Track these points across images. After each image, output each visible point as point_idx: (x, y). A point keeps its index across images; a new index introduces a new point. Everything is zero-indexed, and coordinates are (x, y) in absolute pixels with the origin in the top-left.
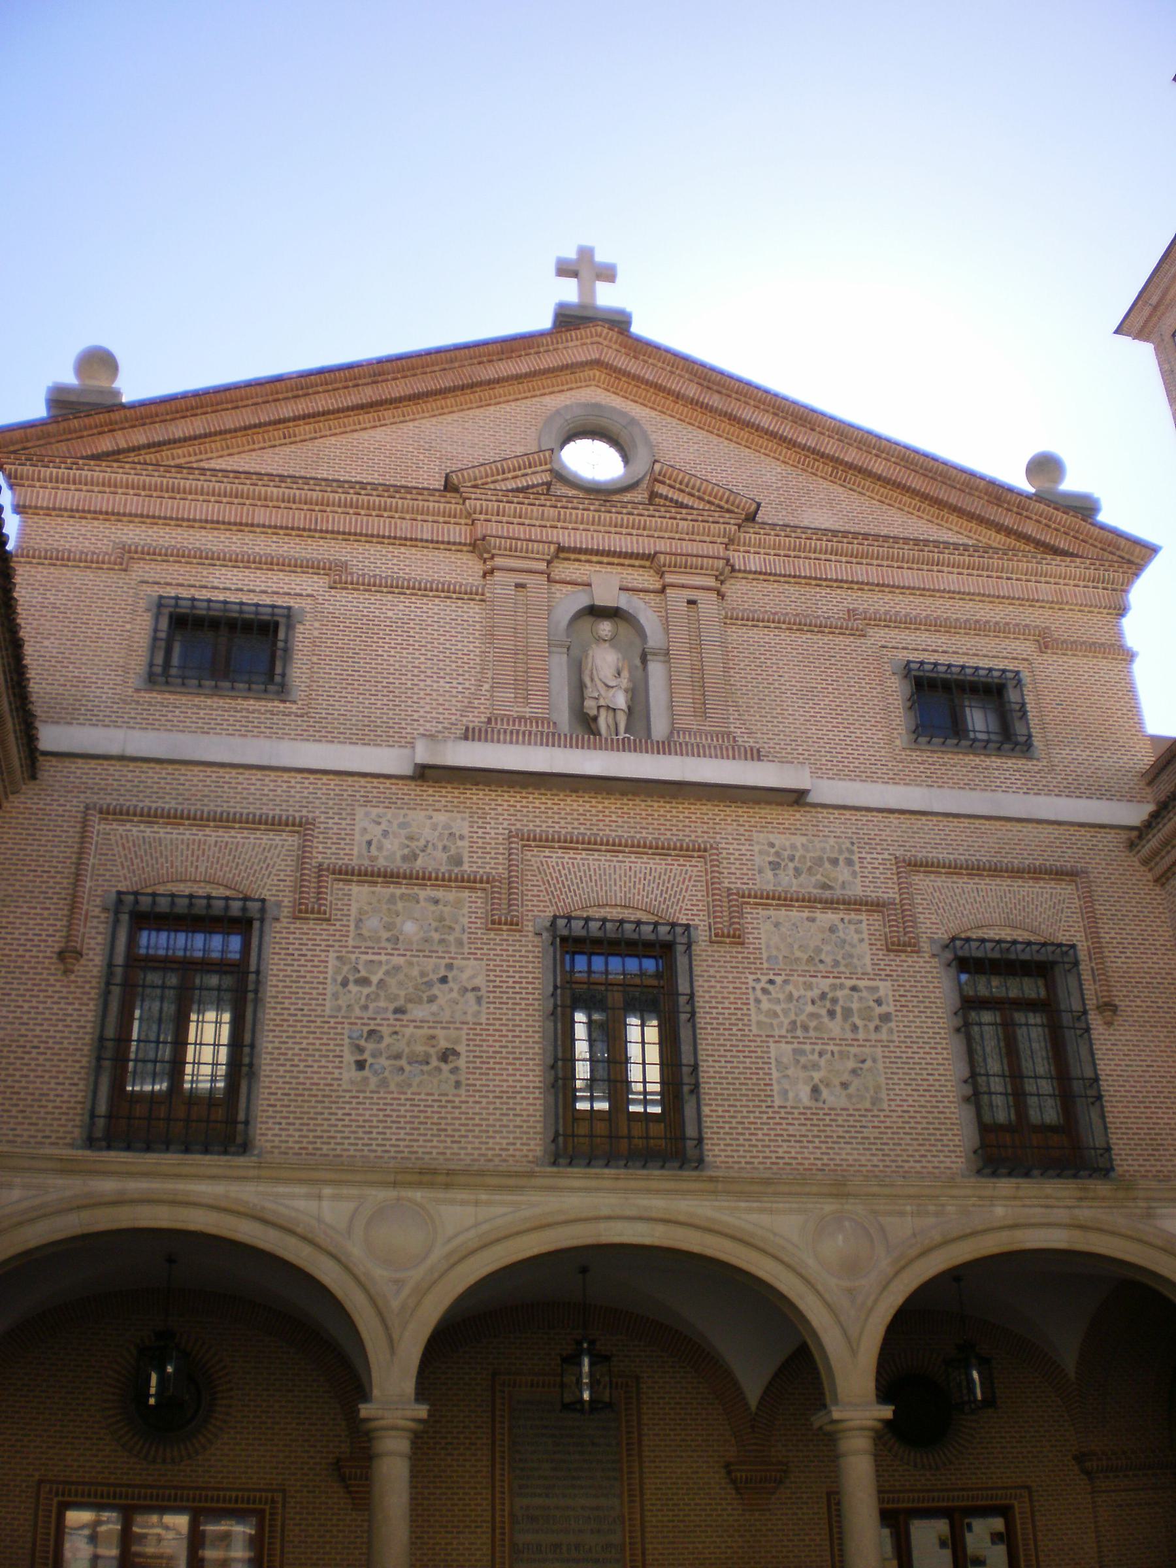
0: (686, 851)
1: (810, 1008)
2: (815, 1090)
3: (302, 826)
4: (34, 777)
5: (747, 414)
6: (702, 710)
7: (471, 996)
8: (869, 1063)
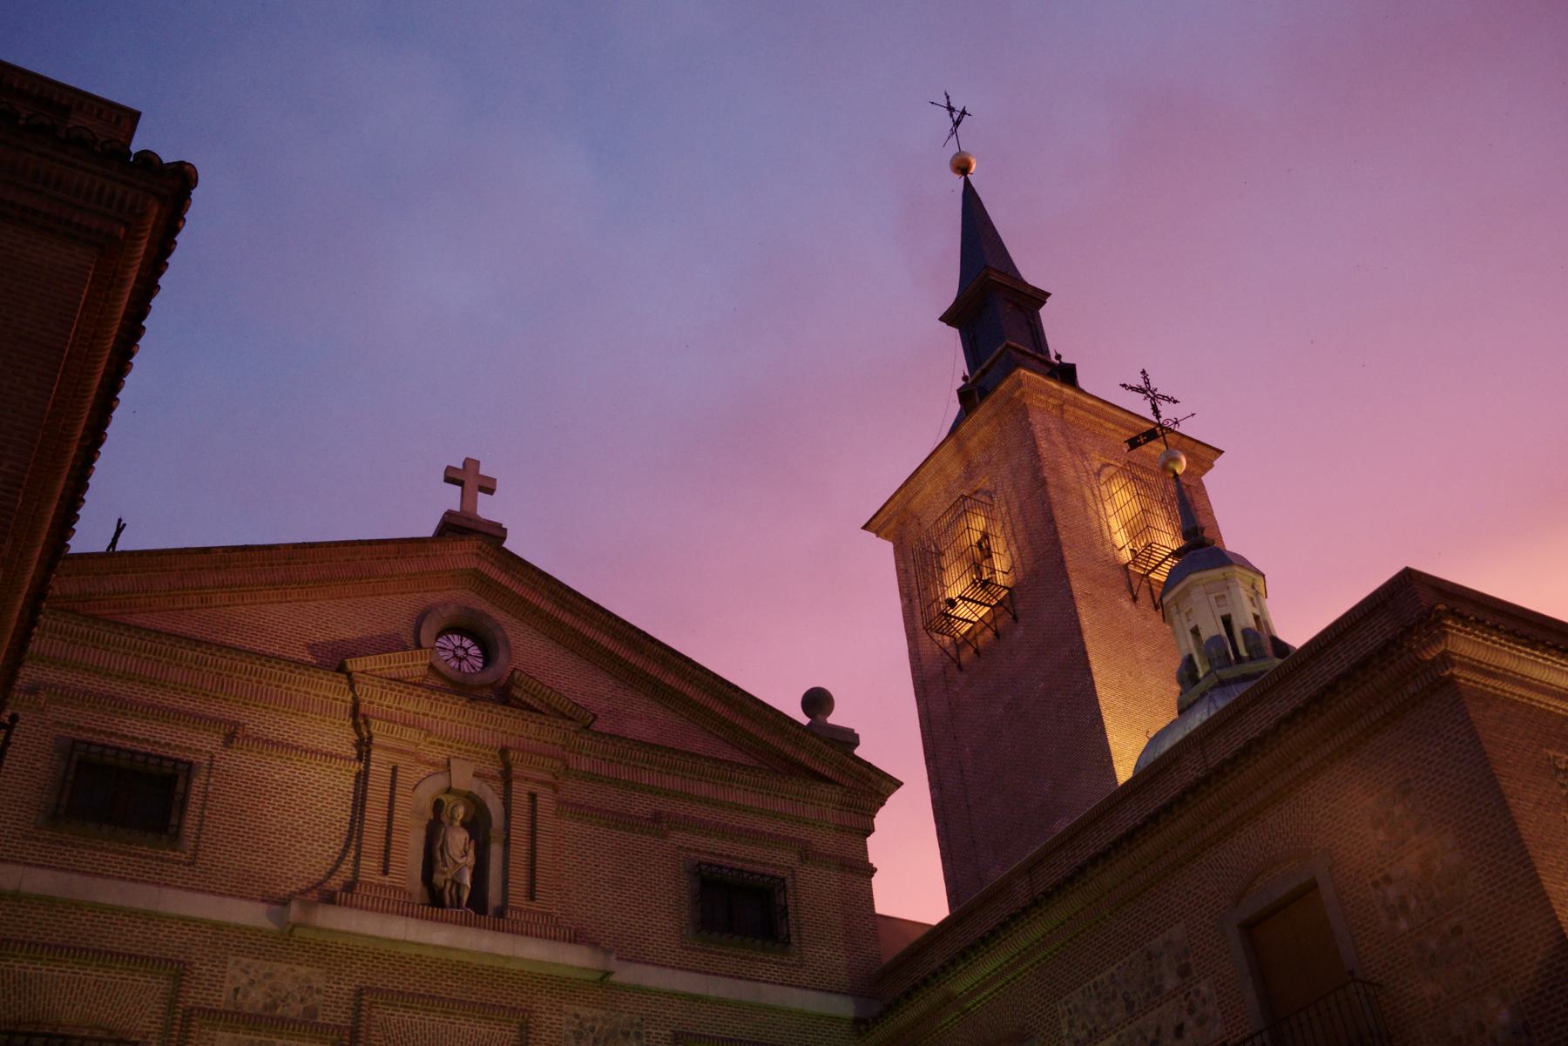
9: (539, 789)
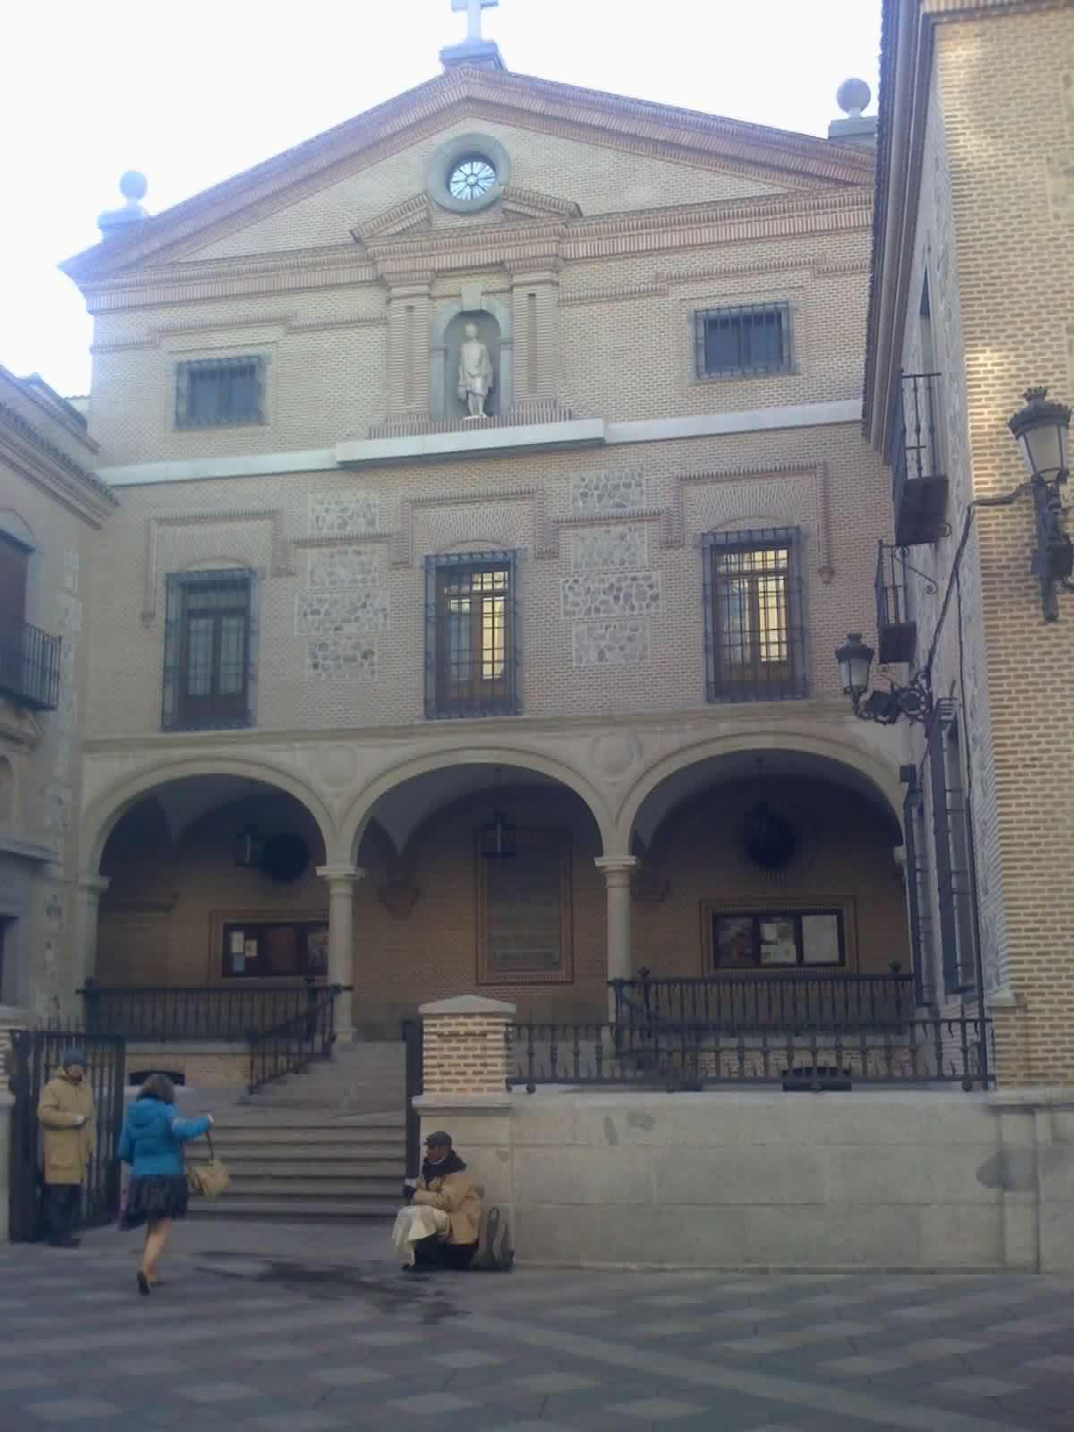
0: (521, 495)
1: (603, 597)
2: (601, 656)
3: (272, 514)
4: (117, 504)
5: (582, 116)
6: (533, 386)
7: (381, 615)
8: (640, 630)
9: (537, 289)
